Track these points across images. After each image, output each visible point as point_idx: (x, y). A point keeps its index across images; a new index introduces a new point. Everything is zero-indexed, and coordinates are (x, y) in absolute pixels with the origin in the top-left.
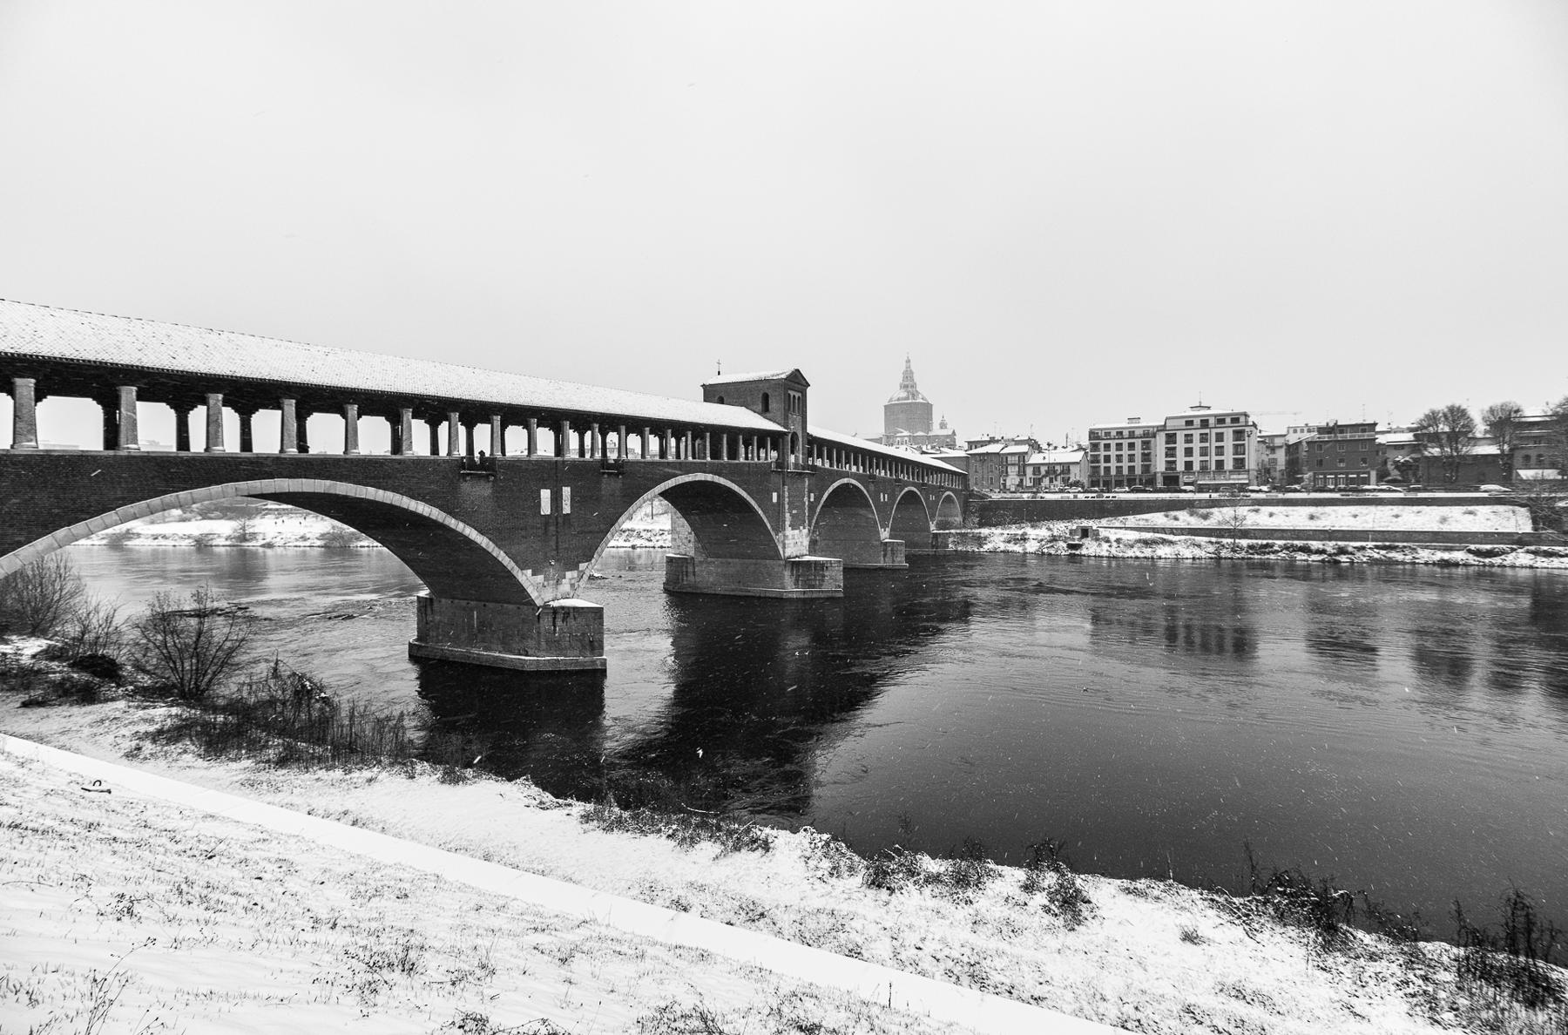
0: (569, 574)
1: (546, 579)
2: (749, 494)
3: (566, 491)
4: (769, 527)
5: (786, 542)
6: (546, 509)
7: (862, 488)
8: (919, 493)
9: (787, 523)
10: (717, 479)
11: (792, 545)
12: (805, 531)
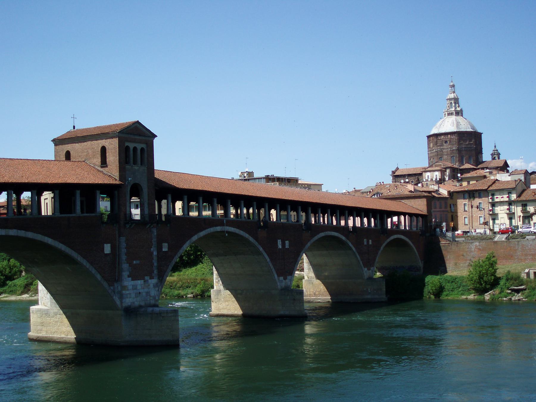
2: (69, 247)
5: (124, 292)
7: (247, 236)
8: (344, 238)
9: (125, 274)
10: (22, 233)
11: (133, 295)
12: (154, 281)
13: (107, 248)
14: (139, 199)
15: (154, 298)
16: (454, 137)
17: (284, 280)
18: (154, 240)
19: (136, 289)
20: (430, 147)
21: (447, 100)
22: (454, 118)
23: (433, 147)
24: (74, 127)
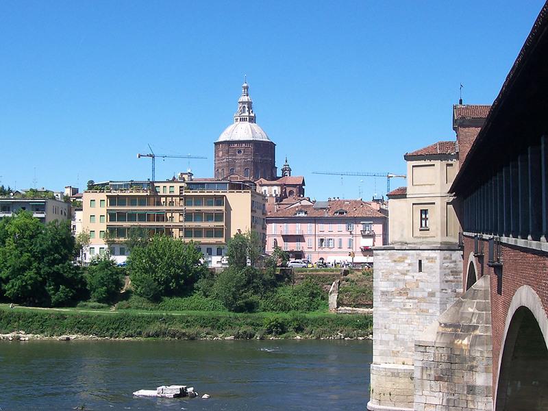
16: (251, 147)
20: (218, 156)
21: (240, 103)
22: (247, 124)
23: (222, 156)
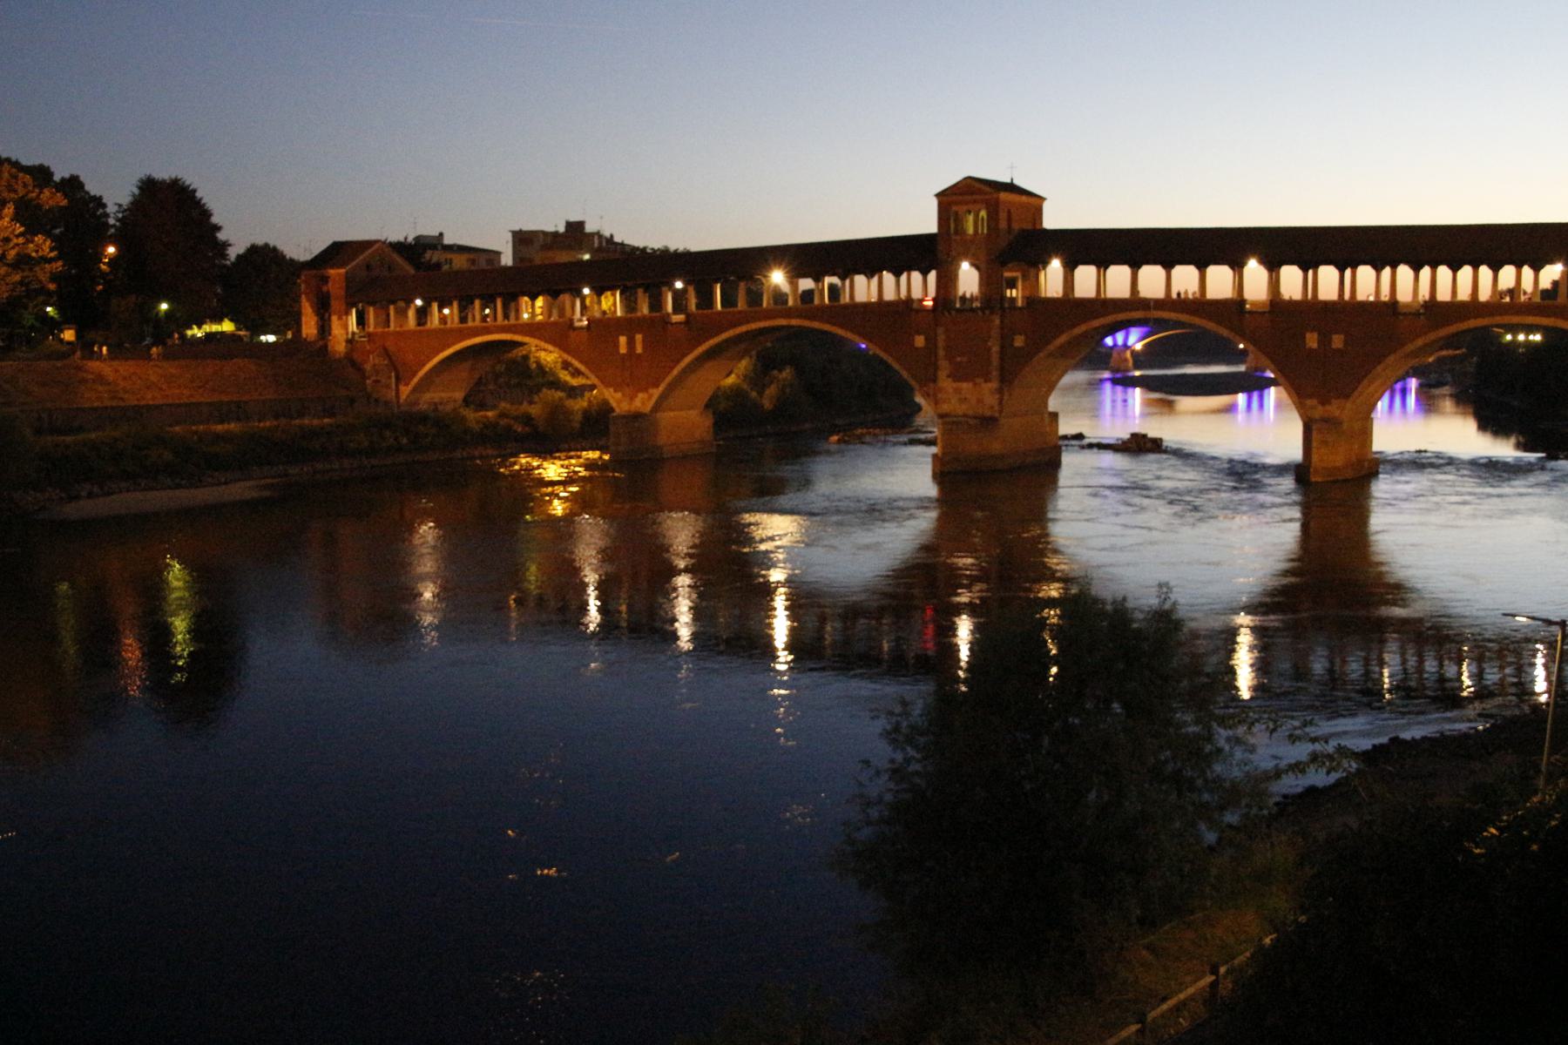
0: (641, 395)
1: (623, 395)
3: (639, 337)
4: (905, 374)
6: (623, 350)
9: (942, 374)
12: (994, 385)
13: (920, 341)
14: (472, 303)
15: (992, 407)
17: (1320, 408)
18: (995, 333)
19: (960, 393)
24: (1012, 180)
